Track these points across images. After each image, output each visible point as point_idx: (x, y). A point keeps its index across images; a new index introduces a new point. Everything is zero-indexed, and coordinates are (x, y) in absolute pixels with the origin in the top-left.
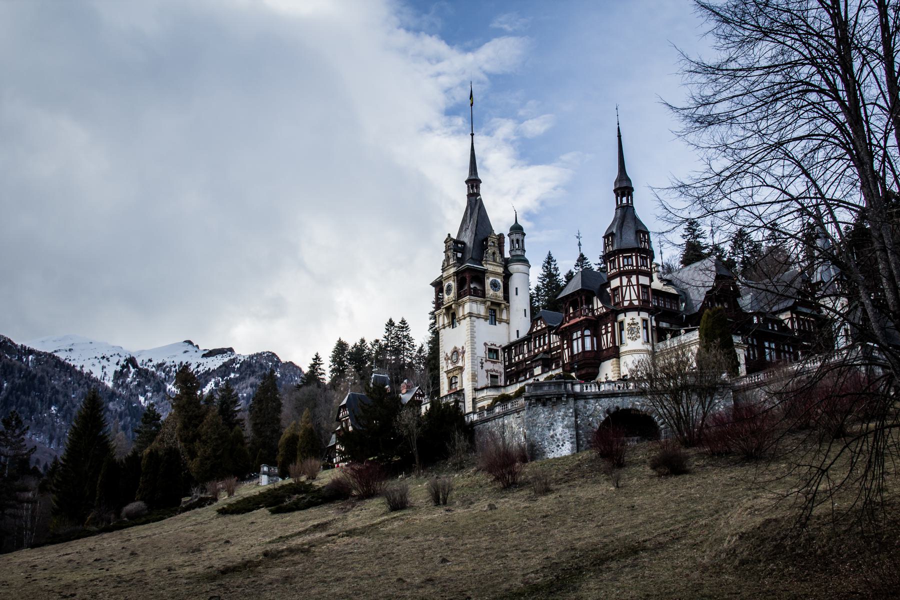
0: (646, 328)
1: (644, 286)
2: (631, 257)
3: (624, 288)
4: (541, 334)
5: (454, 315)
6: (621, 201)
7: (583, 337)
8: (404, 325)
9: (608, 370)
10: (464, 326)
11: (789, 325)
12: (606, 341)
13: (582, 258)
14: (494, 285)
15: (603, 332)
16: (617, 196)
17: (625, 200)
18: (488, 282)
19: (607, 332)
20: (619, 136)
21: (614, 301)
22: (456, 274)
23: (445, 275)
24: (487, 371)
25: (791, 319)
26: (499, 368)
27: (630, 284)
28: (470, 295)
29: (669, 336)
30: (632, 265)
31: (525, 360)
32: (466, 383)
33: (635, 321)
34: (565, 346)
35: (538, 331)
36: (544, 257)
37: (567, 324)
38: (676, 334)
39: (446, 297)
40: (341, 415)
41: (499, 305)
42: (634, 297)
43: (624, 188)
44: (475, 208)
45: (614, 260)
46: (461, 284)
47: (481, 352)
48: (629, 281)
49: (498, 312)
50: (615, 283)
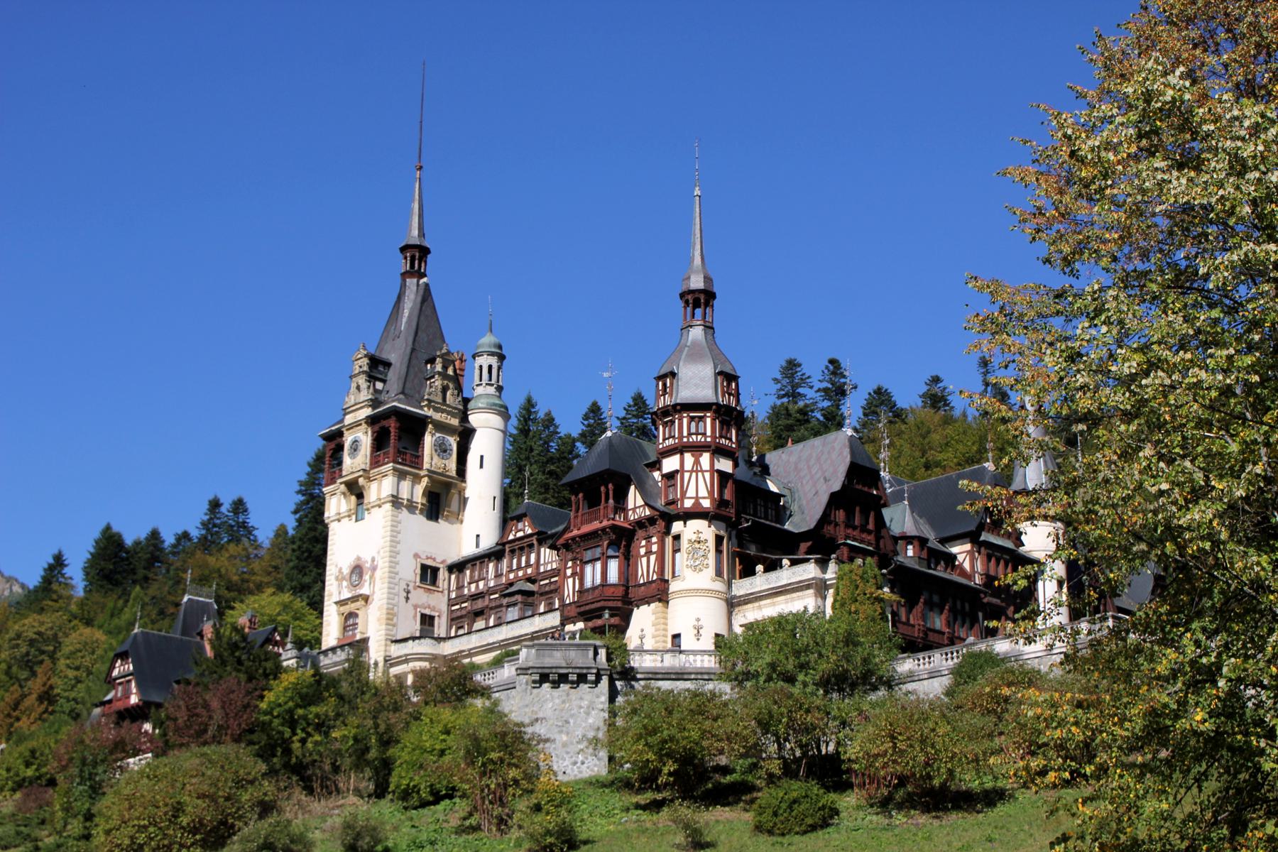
0: (719, 551)
1: (723, 476)
3: (687, 475)
4: (522, 547)
5: (360, 496)
7: (605, 559)
8: (239, 506)
9: (643, 619)
10: (379, 519)
11: (967, 566)
12: (646, 568)
14: (442, 449)
15: (643, 551)
16: (687, 302)
17: (699, 311)
18: (428, 440)
19: (649, 553)
21: (666, 496)
22: (371, 421)
23: (349, 419)
24: (416, 607)
25: (970, 553)
26: (437, 603)
27: (697, 468)
28: (394, 462)
29: (760, 568)
30: (704, 434)
32: (373, 627)
33: (703, 537)
34: (569, 572)
37: (575, 532)
38: (772, 566)
39: (347, 461)
40: (115, 673)
41: (448, 486)
42: (703, 492)
45: (672, 422)
47: (410, 572)
48: (697, 462)
49: (443, 498)
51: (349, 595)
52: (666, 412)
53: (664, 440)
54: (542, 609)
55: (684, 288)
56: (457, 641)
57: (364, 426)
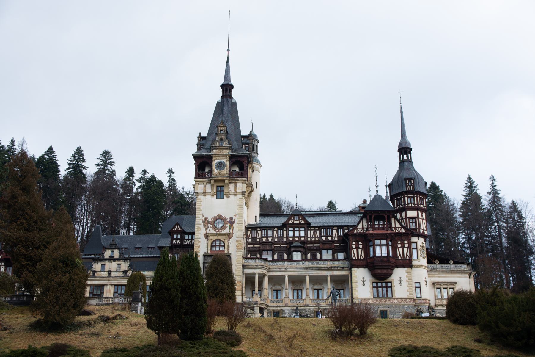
2: (423, 199)
6: (403, 157)
13: (51, 150)
15: (399, 246)
19: (403, 247)
20: (402, 112)
34: (354, 246)
35: (293, 224)
37: (371, 232)
39: (215, 171)
42: (425, 229)
43: (405, 150)
44: (226, 107)
45: (413, 197)
46: (231, 165)
48: (422, 216)
50: (411, 214)
51: (214, 232)
52: (410, 192)
53: (408, 204)
54: (309, 256)
55: (403, 146)
56: (249, 261)
57: (228, 158)
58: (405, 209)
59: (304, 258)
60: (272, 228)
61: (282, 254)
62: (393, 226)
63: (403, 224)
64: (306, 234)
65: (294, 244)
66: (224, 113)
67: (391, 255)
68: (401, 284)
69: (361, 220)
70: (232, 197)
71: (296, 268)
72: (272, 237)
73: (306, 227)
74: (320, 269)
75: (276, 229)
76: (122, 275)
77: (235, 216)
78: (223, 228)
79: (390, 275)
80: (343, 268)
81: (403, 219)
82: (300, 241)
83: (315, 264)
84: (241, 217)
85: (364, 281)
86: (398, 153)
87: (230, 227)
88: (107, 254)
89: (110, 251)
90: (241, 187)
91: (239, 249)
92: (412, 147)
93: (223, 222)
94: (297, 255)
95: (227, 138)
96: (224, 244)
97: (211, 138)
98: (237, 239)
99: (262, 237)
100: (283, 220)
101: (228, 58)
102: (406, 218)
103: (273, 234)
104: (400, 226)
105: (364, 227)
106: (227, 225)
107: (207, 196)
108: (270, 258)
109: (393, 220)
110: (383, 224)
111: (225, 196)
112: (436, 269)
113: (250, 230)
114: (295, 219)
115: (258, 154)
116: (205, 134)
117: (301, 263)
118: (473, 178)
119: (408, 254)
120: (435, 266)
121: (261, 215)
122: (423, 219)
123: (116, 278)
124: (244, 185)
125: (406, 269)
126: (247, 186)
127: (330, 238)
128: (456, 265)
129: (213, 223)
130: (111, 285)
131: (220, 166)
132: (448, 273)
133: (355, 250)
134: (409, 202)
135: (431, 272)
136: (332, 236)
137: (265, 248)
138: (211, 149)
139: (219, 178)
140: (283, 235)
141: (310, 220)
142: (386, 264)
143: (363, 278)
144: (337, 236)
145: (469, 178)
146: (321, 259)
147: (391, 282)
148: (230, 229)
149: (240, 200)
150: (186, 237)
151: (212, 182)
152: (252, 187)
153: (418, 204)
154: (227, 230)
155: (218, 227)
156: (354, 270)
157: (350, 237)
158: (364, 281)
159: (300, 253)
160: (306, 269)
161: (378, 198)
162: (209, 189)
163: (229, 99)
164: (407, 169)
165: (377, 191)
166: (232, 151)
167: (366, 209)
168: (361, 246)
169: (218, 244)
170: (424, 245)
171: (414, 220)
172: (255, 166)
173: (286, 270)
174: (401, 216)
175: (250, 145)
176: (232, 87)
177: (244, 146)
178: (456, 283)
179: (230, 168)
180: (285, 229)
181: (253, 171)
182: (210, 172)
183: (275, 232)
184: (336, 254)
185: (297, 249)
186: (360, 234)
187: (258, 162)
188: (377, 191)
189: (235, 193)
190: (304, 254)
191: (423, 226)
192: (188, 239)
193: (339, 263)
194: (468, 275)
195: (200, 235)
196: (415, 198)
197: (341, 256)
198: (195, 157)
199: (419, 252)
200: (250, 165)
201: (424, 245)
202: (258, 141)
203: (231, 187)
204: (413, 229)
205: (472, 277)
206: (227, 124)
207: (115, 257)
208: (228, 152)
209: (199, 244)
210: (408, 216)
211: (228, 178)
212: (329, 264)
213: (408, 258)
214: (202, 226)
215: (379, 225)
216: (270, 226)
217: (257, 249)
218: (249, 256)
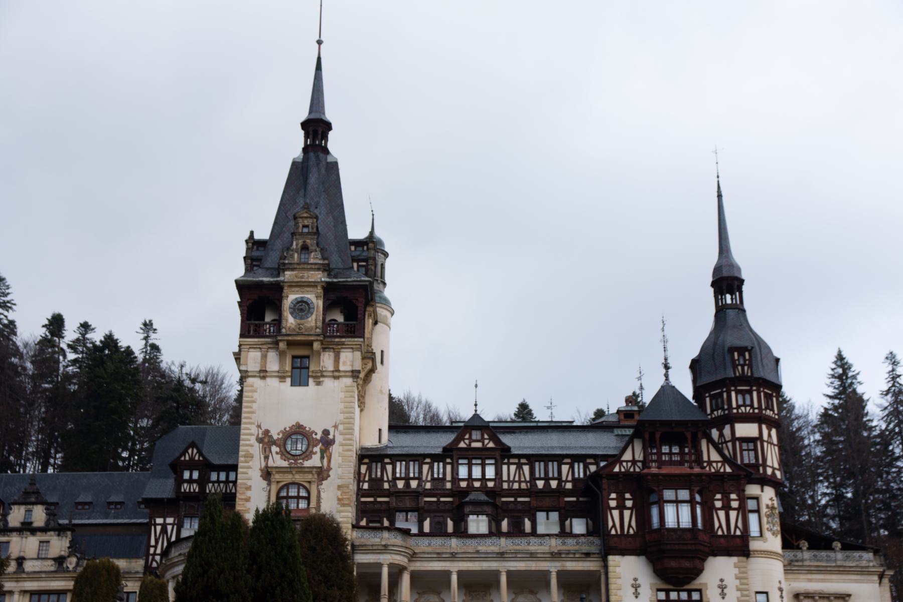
3: (765, 444)
15: (718, 504)
19: (727, 508)
20: (720, 196)
29: (804, 544)
31: (429, 493)
34: (613, 504)
35: (469, 449)
36: (827, 364)
37: (654, 470)
39: (290, 321)
42: (776, 466)
43: (727, 282)
45: (750, 392)
46: (327, 308)
48: (770, 435)
50: (746, 430)
51: (285, 464)
52: (743, 380)
53: (738, 407)
54: (505, 524)
55: (725, 273)
57: (320, 290)
58: (733, 419)
59: (494, 530)
60: (419, 458)
61: (441, 519)
62: (705, 458)
63: (726, 452)
64: (498, 472)
65: (472, 497)
66: (309, 187)
67: (700, 525)
68: (723, 595)
69: (630, 442)
70: (328, 383)
71: (478, 552)
72: (419, 478)
73: (498, 458)
74: (532, 556)
75: (428, 460)
76: (53, 569)
77: (336, 427)
78: (307, 455)
79: (699, 571)
80: (588, 555)
81: (726, 442)
82: (484, 489)
83: (520, 544)
84: (349, 430)
85: (636, 587)
86: (712, 290)
87: (323, 452)
88: (16, 516)
89: (23, 509)
90: (350, 359)
91: (343, 505)
92: (744, 276)
93: (305, 442)
94: (478, 522)
95: (318, 245)
96: (308, 492)
97: (279, 244)
98: (339, 482)
99: (395, 479)
100: (445, 440)
101: (319, 59)
102: (734, 439)
103: (420, 472)
104: (719, 458)
105: (637, 458)
106: (317, 449)
107: (268, 380)
108: (415, 530)
109: (704, 443)
110: (682, 453)
111: (311, 381)
112: (802, 560)
113: (366, 461)
114: (474, 437)
115: (384, 284)
116: (263, 233)
117: (489, 541)
118: (849, 358)
119: (740, 524)
120: (799, 554)
121: (391, 428)
122: (772, 444)
123: (35, 576)
124: (358, 354)
125: (735, 559)
126: (363, 358)
127: (554, 484)
128: (848, 553)
129: (282, 444)
130: (24, 592)
131: (302, 308)
132: (831, 572)
133: (616, 513)
134: (741, 402)
135: (790, 568)
136: (559, 479)
137: (400, 505)
138: (280, 269)
139: (299, 338)
140: (444, 473)
141: (507, 440)
142: (690, 547)
143: (635, 580)
144: (570, 478)
145: (840, 358)
146: (534, 533)
147: (700, 591)
148: (322, 458)
149: (348, 390)
150: (214, 476)
151: (282, 345)
152: (373, 360)
153: (760, 407)
154: (315, 461)
155: (293, 452)
156: (613, 560)
157: (605, 481)
158: (636, 587)
159: (484, 518)
160: (501, 556)
161: (668, 392)
162: (273, 365)
163: (321, 155)
164: (734, 327)
165: (666, 376)
166: (329, 276)
167: (644, 417)
168: (629, 504)
169: (293, 492)
170: (776, 505)
171: (751, 446)
172: (381, 312)
173: (453, 557)
174: (721, 435)
175: (371, 262)
176: (328, 126)
177: (355, 265)
178: (849, 596)
179: (324, 314)
180: (449, 460)
181: (376, 323)
182: (278, 323)
183: (425, 468)
184: (568, 522)
185: (478, 508)
186: (627, 476)
187: (386, 302)
188: (666, 376)
189: (336, 374)
190: (495, 521)
191: (773, 458)
192: (218, 482)
193: (578, 543)
194: (876, 578)
195: (250, 471)
196: (755, 394)
197: (579, 526)
198: (241, 286)
199: (764, 520)
200: (370, 309)
201: (776, 505)
202: (386, 255)
203: (327, 361)
204: (749, 465)
205: (886, 581)
206: (317, 212)
207: (35, 525)
208: (320, 277)
209: (249, 493)
210: (738, 435)
211: (321, 338)
212: (554, 544)
213: (738, 533)
214: (256, 449)
215: (671, 454)
216: (415, 452)
217: (384, 507)
218: (363, 523)
